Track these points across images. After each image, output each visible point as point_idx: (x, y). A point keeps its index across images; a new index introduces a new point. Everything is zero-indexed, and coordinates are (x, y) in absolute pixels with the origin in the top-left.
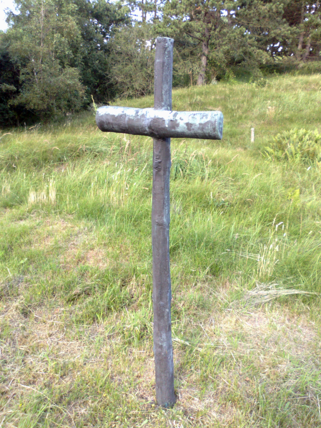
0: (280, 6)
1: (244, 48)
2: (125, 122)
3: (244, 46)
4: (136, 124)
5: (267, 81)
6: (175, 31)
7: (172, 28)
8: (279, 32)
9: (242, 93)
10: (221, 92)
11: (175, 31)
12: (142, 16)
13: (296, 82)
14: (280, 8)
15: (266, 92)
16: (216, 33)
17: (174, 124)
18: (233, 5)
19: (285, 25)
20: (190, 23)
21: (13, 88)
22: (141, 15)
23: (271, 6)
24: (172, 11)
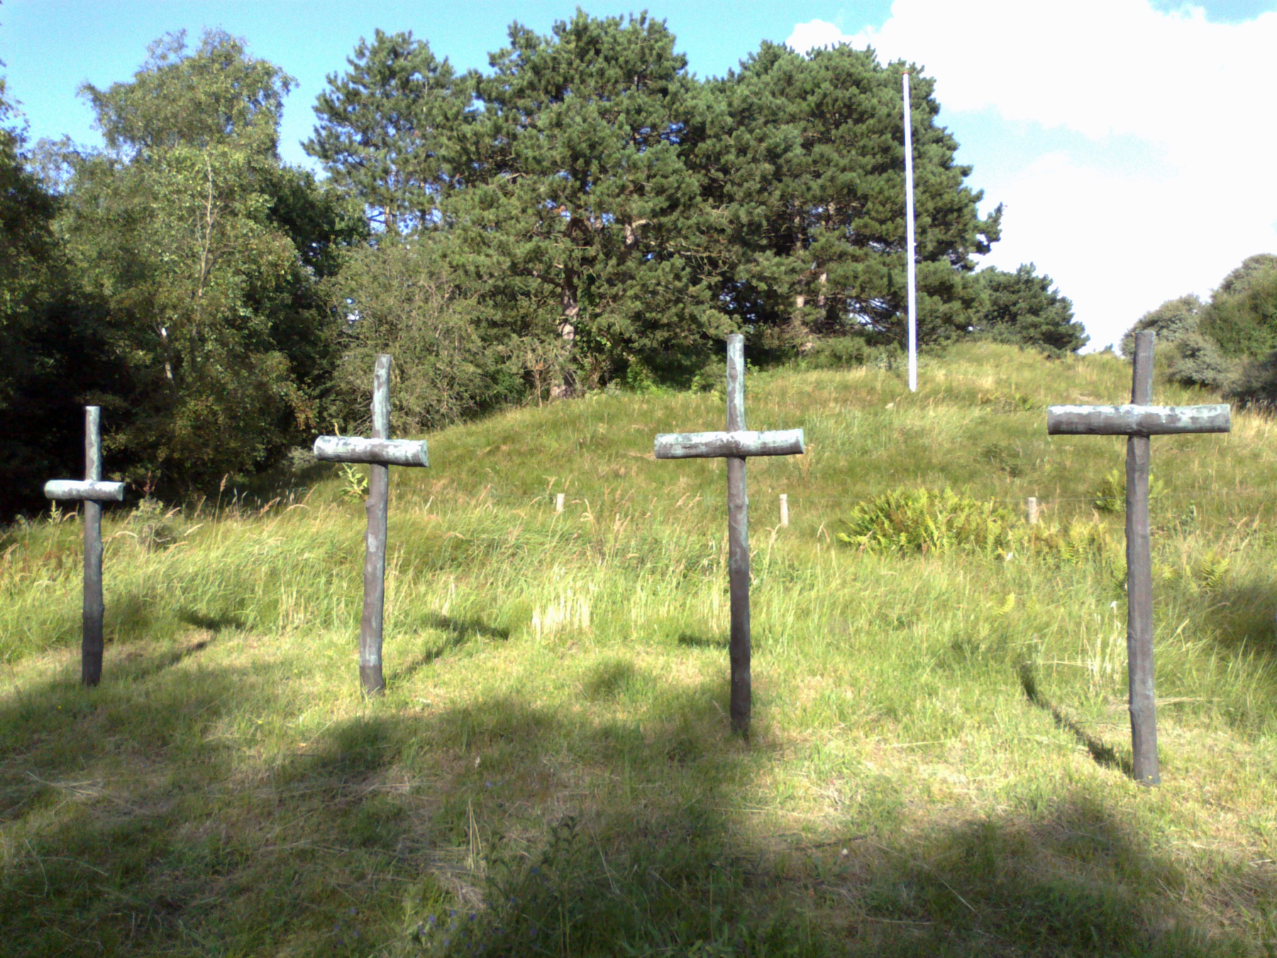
0: (758, 210)
1: (681, 305)
2: (1096, 422)
3: (678, 301)
4: (1117, 422)
6: (499, 263)
7: (487, 255)
8: (758, 268)
10: (644, 414)
11: (499, 263)
13: (819, 385)
14: (759, 215)
16: (609, 269)
18: (651, 204)
19: (769, 253)
20: (543, 244)
23: (737, 210)
24: (486, 213)
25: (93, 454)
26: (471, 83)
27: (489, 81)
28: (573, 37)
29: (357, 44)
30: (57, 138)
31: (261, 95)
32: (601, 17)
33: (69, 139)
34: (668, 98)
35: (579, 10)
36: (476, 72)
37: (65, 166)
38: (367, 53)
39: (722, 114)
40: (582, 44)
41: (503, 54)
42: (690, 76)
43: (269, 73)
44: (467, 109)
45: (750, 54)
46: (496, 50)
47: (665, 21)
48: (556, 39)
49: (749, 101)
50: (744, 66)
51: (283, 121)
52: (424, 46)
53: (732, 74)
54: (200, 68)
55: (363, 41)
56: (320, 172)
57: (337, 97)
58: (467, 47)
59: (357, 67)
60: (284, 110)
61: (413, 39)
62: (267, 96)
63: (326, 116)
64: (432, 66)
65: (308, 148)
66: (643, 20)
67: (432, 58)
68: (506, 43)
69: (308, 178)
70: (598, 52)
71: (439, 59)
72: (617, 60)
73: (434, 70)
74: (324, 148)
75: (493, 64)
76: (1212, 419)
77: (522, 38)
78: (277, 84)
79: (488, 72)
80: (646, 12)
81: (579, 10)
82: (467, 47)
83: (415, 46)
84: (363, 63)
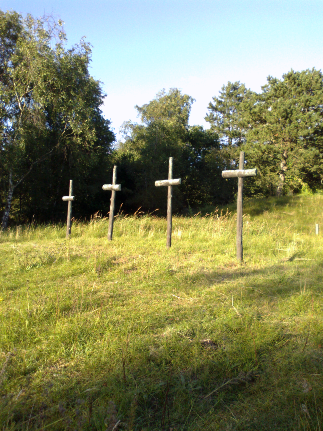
12: (229, 141)
17: (244, 172)
21: (130, 191)
22: (227, 140)
25: (71, 190)
27: (260, 95)
28: (288, 79)
29: (222, 86)
30: (128, 120)
31: (185, 104)
32: (301, 72)
33: (130, 120)
35: (292, 69)
37: (130, 128)
38: (225, 89)
40: (290, 80)
41: (266, 86)
43: (188, 98)
46: (263, 85)
48: (283, 80)
51: (191, 112)
52: (243, 85)
55: (224, 85)
56: (207, 126)
57: (214, 104)
58: (256, 85)
59: (222, 93)
60: (192, 109)
61: (240, 83)
62: (187, 105)
63: (211, 110)
64: (245, 91)
65: (206, 118)
66: (313, 70)
67: (245, 89)
68: (267, 83)
69: (201, 128)
70: (295, 83)
71: (248, 89)
72: (301, 84)
73: (245, 93)
74: (210, 119)
75: (262, 90)
76: (252, 172)
78: (190, 101)
79: (260, 92)
80: (314, 68)
82: (256, 85)
83: (241, 85)
84: (222, 92)
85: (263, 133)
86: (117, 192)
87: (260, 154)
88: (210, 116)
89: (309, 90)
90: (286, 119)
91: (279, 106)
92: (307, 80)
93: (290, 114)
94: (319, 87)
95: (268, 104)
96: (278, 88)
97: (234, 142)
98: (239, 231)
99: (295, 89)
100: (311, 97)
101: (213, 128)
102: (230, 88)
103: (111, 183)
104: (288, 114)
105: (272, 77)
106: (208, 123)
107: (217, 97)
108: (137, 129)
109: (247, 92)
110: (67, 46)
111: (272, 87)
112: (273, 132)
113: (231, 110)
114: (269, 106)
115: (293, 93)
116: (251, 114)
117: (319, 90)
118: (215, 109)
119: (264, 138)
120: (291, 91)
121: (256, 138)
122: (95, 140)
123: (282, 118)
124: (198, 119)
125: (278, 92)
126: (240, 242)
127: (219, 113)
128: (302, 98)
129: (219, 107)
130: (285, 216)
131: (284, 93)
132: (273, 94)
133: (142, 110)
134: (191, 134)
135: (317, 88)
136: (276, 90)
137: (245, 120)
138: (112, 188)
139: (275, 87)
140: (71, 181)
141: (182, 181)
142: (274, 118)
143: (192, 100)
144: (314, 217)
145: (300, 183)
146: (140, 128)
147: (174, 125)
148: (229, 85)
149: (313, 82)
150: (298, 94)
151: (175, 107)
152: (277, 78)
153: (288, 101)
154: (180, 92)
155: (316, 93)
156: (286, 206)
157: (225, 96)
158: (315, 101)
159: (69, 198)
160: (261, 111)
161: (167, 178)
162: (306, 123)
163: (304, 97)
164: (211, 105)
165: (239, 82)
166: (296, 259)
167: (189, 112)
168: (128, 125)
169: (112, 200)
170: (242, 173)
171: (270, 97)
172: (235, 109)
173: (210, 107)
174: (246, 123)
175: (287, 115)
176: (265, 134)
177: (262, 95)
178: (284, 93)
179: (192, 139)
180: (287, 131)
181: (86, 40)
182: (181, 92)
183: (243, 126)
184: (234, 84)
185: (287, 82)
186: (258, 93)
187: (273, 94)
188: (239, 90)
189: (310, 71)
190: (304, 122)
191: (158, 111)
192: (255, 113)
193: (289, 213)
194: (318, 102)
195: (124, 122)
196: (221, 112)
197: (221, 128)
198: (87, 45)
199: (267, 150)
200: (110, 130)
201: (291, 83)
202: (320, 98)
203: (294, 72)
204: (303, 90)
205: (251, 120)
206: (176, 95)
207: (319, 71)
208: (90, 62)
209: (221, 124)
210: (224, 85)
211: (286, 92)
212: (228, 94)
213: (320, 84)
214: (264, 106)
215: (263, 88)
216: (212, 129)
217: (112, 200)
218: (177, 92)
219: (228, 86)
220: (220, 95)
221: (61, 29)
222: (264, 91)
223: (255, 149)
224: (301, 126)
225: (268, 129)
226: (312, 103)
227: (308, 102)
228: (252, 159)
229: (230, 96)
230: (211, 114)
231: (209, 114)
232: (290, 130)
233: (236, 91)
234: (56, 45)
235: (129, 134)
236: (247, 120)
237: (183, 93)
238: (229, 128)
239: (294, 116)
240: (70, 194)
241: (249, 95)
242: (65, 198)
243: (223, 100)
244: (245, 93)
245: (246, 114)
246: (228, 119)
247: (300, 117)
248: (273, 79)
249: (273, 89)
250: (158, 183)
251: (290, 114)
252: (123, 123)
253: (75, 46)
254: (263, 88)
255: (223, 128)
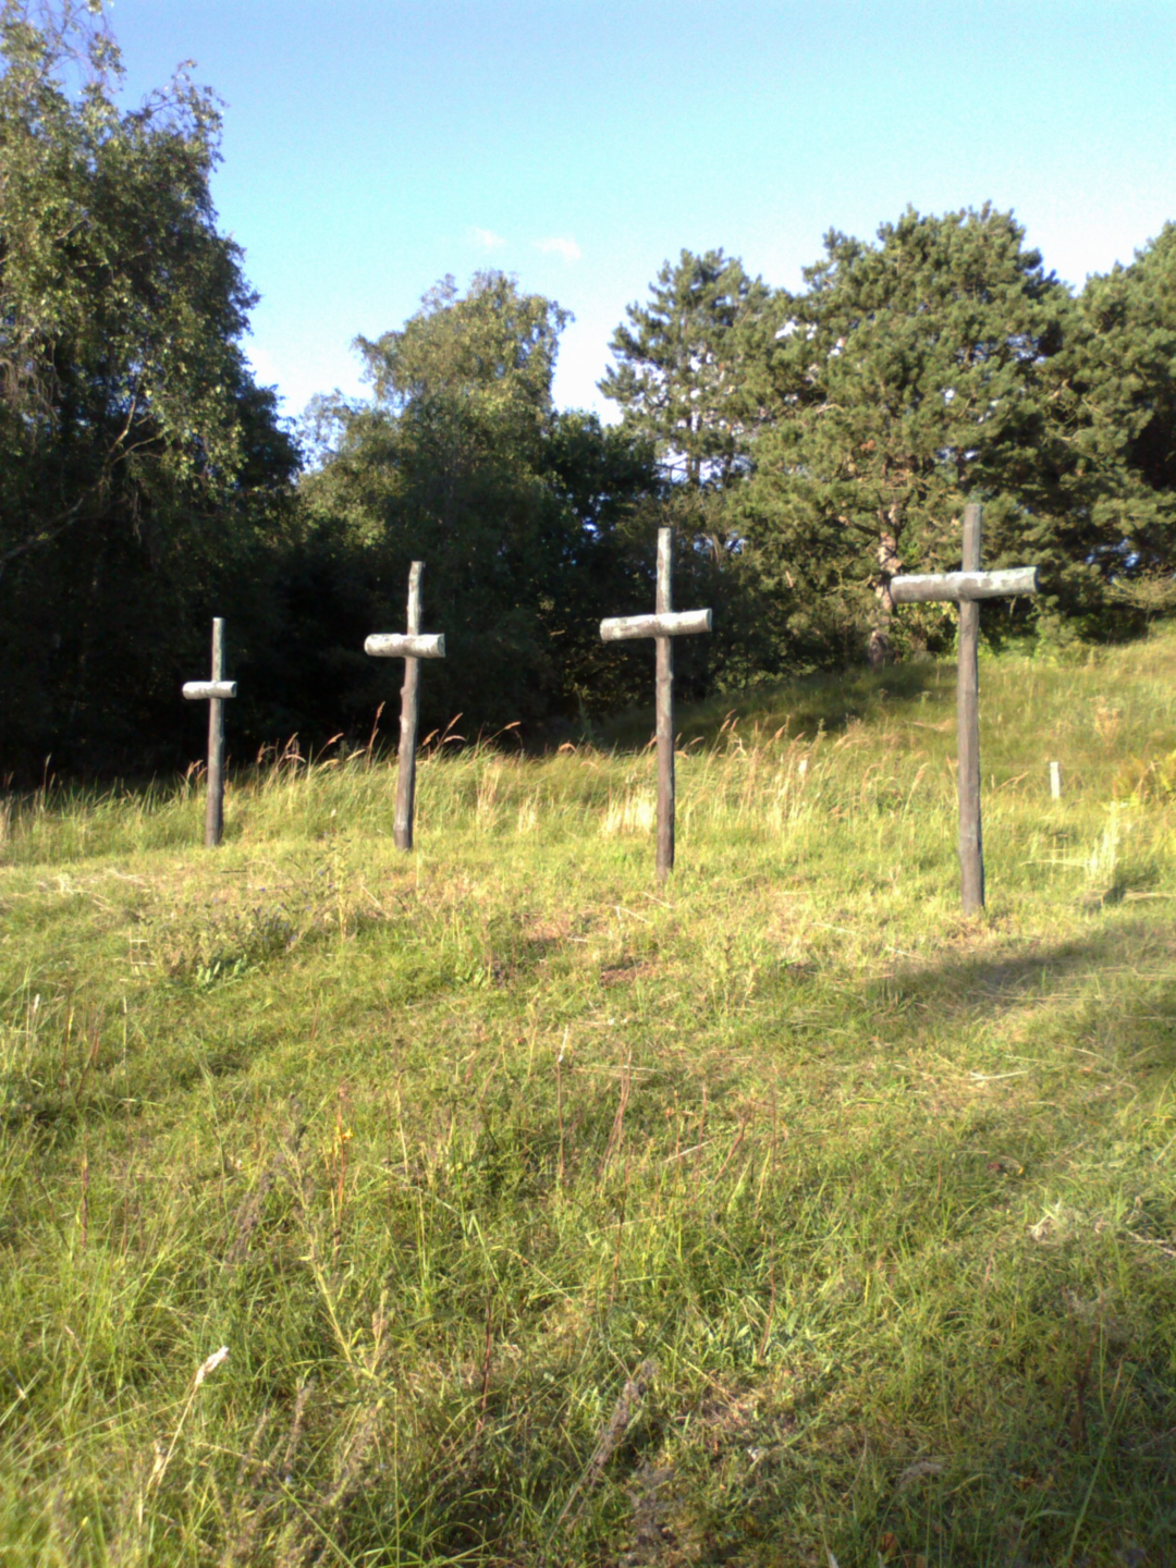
2: (928, 589)
4: (943, 588)
5: (1093, 649)
9: (1014, 683)
12: (689, 469)
15: (1091, 678)
17: (987, 582)
22: (683, 465)
25: (217, 658)
26: (781, 303)
27: (801, 300)
28: (898, 242)
29: (661, 268)
30: (329, 393)
32: (941, 218)
33: (338, 392)
34: (1007, 305)
35: (910, 208)
36: (784, 291)
37: (336, 421)
38: (671, 277)
39: (1080, 319)
40: (907, 248)
41: (820, 269)
42: (1046, 274)
43: (544, 308)
44: (779, 335)
45: (1149, 240)
46: (811, 264)
47: (1012, 212)
48: (880, 246)
49: (1111, 301)
50: (1140, 256)
51: (557, 360)
52: (736, 264)
53: (1118, 269)
54: (475, 310)
55: (667, 263)
56: (611, 415)
57: (635, 333)
58: (782, 261)
59: (660, 294)
60: (560, 349)
62: (542, 334)
63: (622, 353)
64: (743, 286)
65: (603, 387)
66: (986, 211)
67: (745, 279)
68: (821, 254)
69: (593, 421)
70: (925, 257)
71: (753, 278)
72: (948, 262)
73: (745, 291)
75: (807, 281)
76: (1018, 581)
77: (843, 249)
78: (552, 319)
79: (799, 288)
81: (910, 208)
82: (782, 261)
83: (726, 264)
84: (664, 289)
85: (819, 437)
86: (425, 663)
87: (811, 513)
88: (622, 376)
89: (976, 283)
90: (901, 388)
91: (876, 340)
92: (966, 247)
93: (916, 370)
94: (1012, 272)
95: (830, 331)
96: (865, 273)
97: (706, 472)
98: (971, 802)
99: (928, 280)
100: (983, 308)
101: (632, 419)
102: (687, 276)
103: (403, 630)
104: (907, 369)
105: (840, 234)
106: (614, 402)
107: (644, 307)
108: (361, 423)
109: (752, 291)
110: (126, 100)
111: (843, 271)
112: (852, 434)
113: (694, 353)
114: (832, 339)
115: (919, 293)
116: (771, 369)
117: (1009, 283)
118: (636, 351)
119: (822, 456)
120: (913, 284)
121: (794, 457)
122: (239, 466)
123: (887, 383)
124: (581, 387)
125: (866, 288)
126: (975, 844)
127: (653, 368)
128: (954, 312)
129: (652, 343)
130: (920, 735)
131: (888, 292)
132: (849, 297)
133: (385, 355)
134: (559, 445)
135: (1003, 277)
136: (857, 282)
137: (750, 392)
138: (407, 651)
139: (854, 270)
140: (217, 622)
141: (715, 617)
142: (860, 384)
143: (561, 316)
144: (1028, 738)
145: (947, 618)
146: (377, 420)
147: (508, 409)
148: (686, 257)
149: (991, 256)
150: (937, 298)
151: (500, 343)
152: (859, 239)
153: (905, 325)
154: (513, 285)
155: (1003, 296)
156: (919, 700)
157: (671, 304)
158: (999, 322)
159: (218, 686)
160: (806, 357)
161: (651, 608)
162: (973, 402)
163: (960, 307)
164: (622, 334)
165: (721, 251)
166: (1130, 895)
167: (550, 361)
168: (328, 409)
169: (408, 693)
170: (979, 585)
171: (838, 307)
172: (709, 349)
173: (622, 343)
174: (751, 402)
175: (905, 375)
176: (826, 441)
177: (809, 298)
178: (888, 292)
179: (565, 462)
180: (905, 431)
181: (199, 79)
182: (517, 289)
183: (740, 414)
184: (703, 258)
185: (898, 252)
186: (794, 294)
187: (849, 297)
188: (721, 284)
189: (973, 215)
190: (967, 396)
191: (443, 358)
192: (785, 365)
193: (932, 726)
194: (1010, 326)
195: (314, 400)
196: (659, 363)
197: (661, 419)
198: (201, 95)
199: (835, 500)
200: (280, 426)
201: (913, 257)
202: (1018, 313)
203: (920, 219)
204: (953, 284)
205: (769, 390)
206: (501, 297)
207: (1008, 218)
208: (217, 163)
209: (661, 404)
210: (667, 263)
211: (894, 289)
212: (684, 298)
213: (1014, 263)
214: (817, 340)
215: (808, 273)
216: (630, 426)
217: (408, 693)
218: (503, 284)
219: (681, 267)
220: (655, 299)
221: (98, 26)
222: (815, 285)
223: (793, 497)
224: (954, 412)
225: (838, 423)
226: (987, 331)
227: (976, 327)
228: (782, 532)
229: (689, 303)
230: (624, 367)
231: (617, 371)
232: (917, 428)
233: (711, 285)
234: (88, 89)
235: (332, 445)
236: (756, 390)
237: (523, 290)
238: (689, 422)
239: (931, 378)
240: (217, 672)
241: (755, 302)
242: (192, 689)
243: (665, 319)
244: (745, 291)
245: (749, 371)
246: (684, 389)
247: (950, 379)
248: (845, 240)
249: (846, 279)
250: (613, 628)
251: (916, 370)
252: (307, 401)
253: (156, 100)
254: (808, 273)
255: (670, 420)
